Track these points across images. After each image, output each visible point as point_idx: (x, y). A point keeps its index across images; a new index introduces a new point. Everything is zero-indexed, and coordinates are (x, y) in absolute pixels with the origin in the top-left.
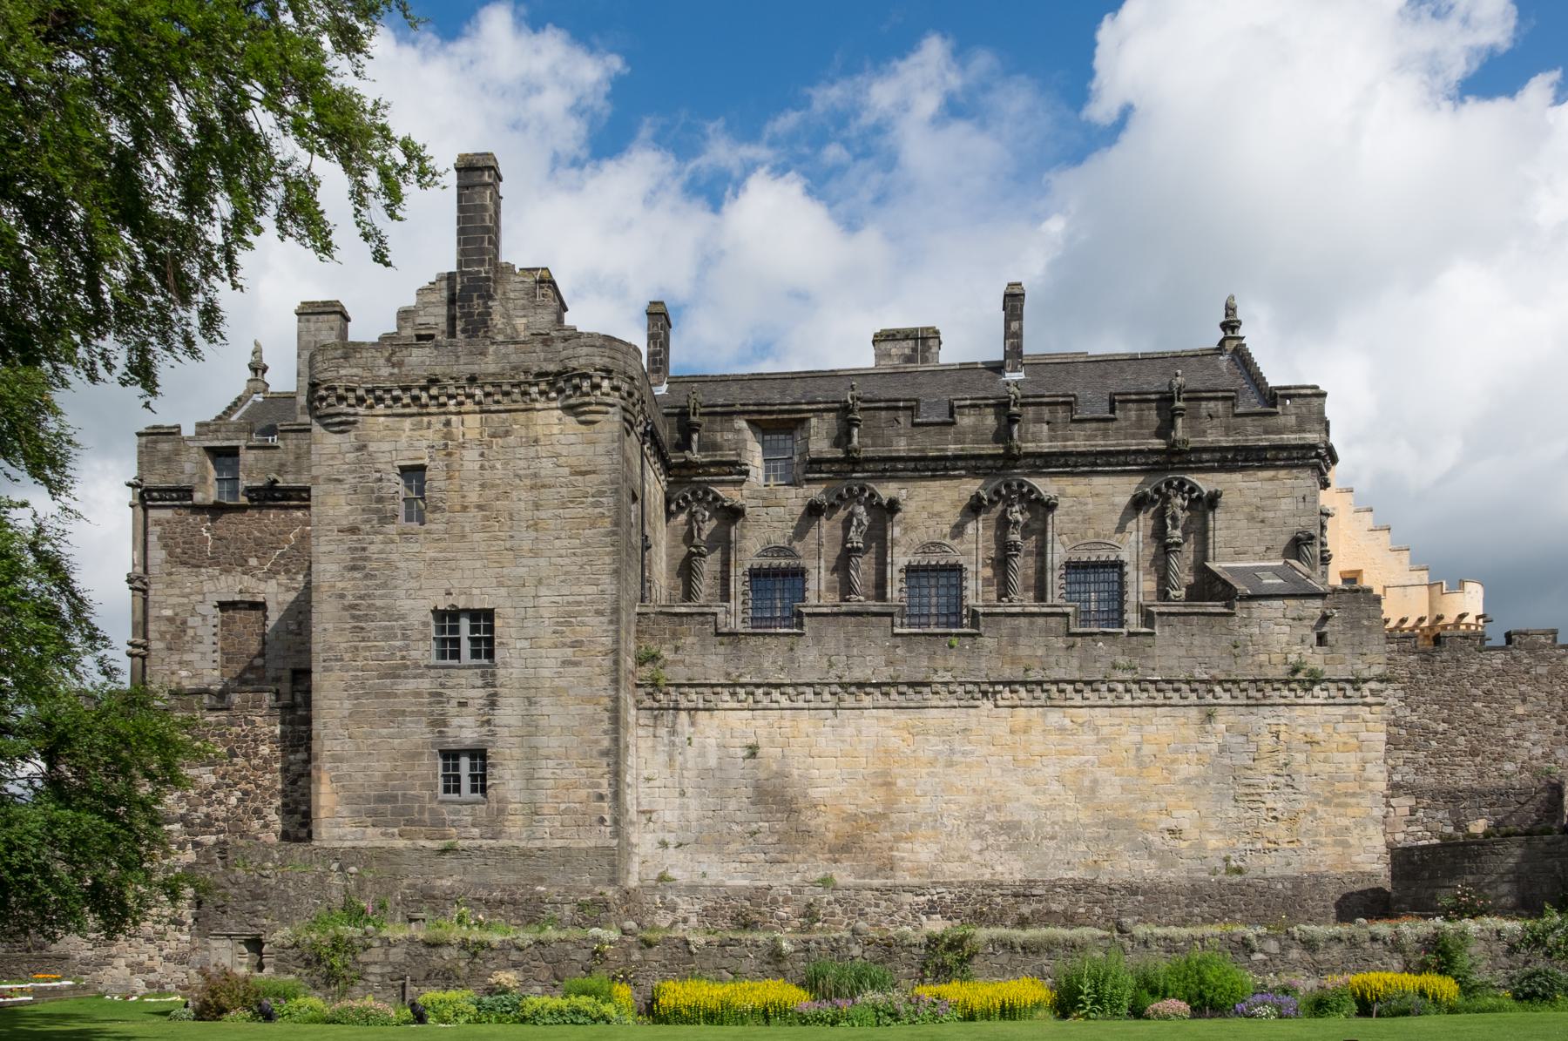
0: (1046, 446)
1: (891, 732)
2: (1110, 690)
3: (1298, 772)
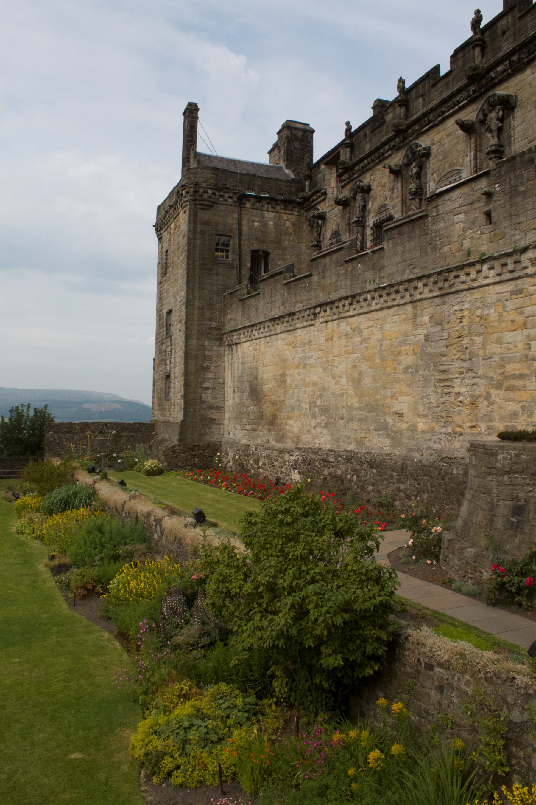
0: (419, 114)
1: (286, 347)
2: (365, 300)
3: (477, 356)
